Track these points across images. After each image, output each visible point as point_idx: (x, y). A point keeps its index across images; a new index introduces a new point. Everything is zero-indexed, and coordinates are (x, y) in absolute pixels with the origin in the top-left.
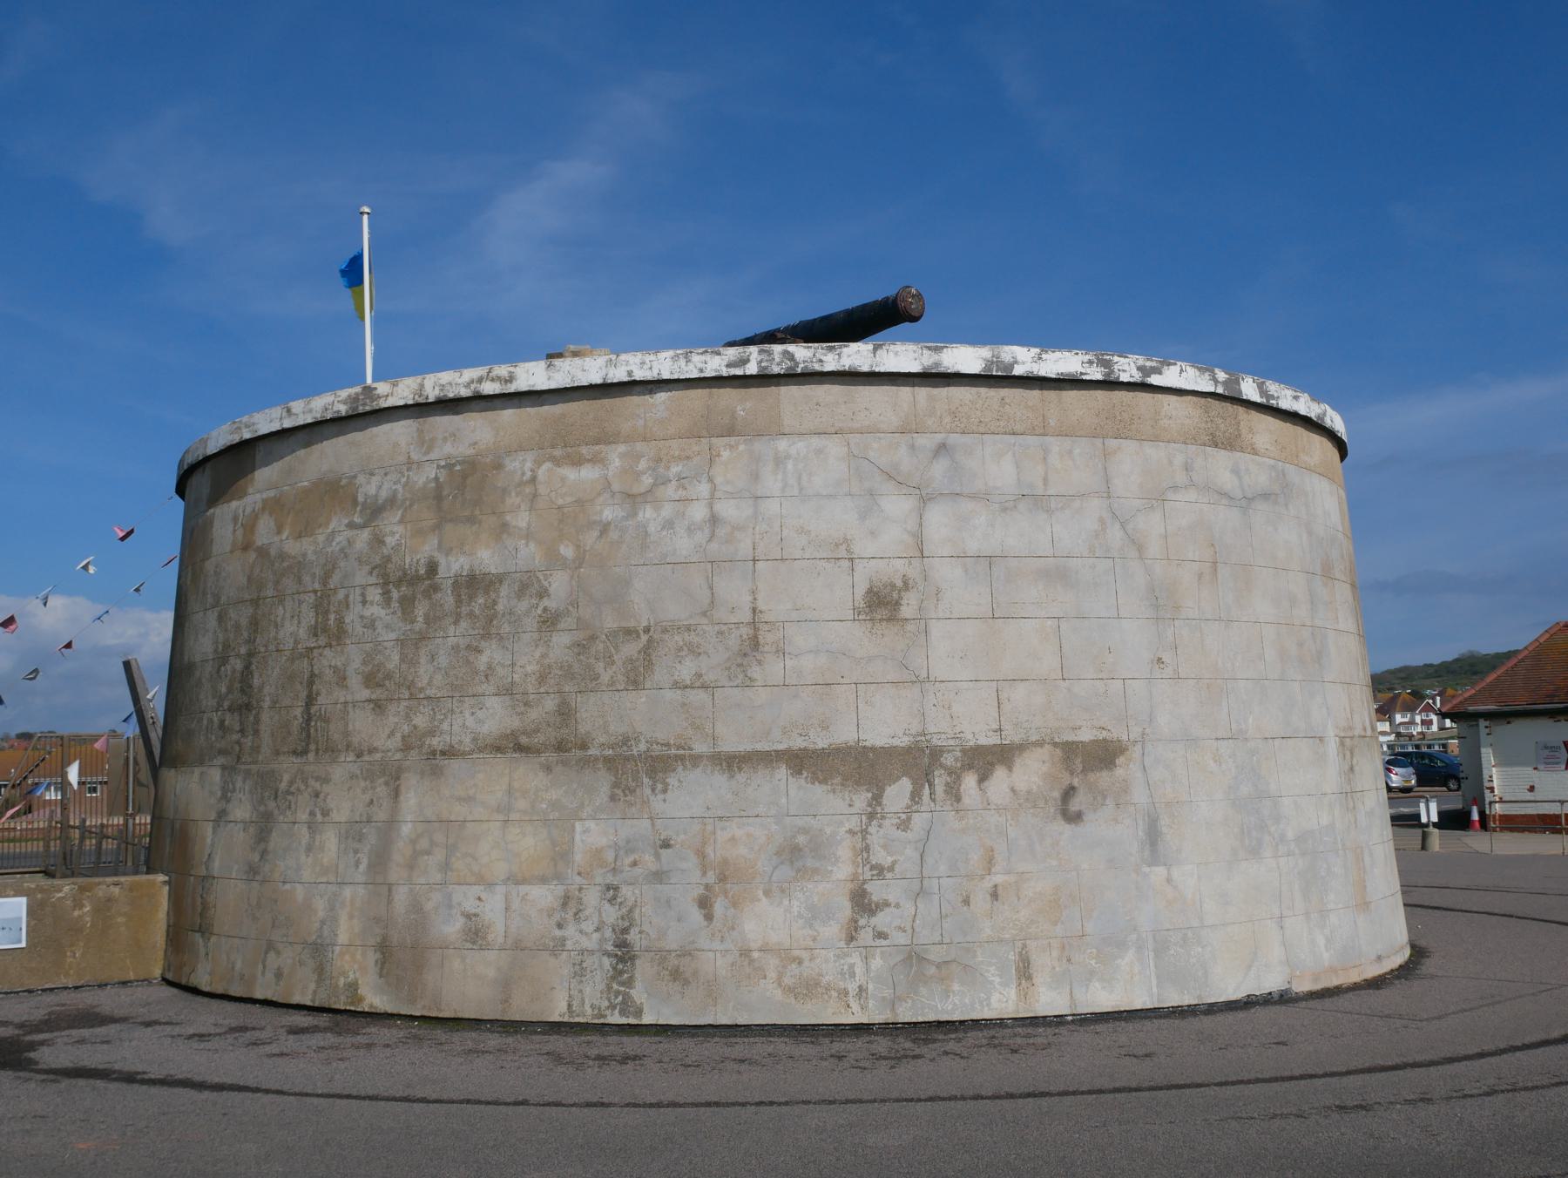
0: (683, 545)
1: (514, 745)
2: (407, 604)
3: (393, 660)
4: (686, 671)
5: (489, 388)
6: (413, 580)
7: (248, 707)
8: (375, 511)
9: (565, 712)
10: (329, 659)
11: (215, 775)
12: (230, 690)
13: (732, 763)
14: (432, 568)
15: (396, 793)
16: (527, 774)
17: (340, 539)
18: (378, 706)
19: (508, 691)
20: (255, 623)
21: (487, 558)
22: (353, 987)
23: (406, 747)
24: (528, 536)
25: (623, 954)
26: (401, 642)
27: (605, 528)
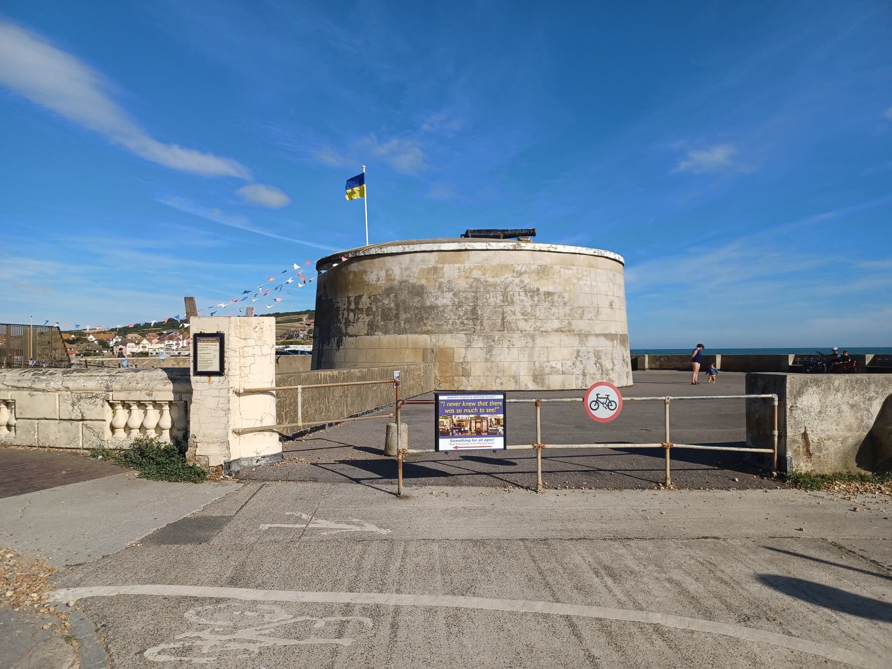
0: (587, 290)
1: (559, 330)
2: (532, 297)
3: (529, 310)
4: (589, 316)
5: (551, 249)
6: (534, 292)
7: (477, 319)
8: (521, 274)
9: (570, 323)
10: (508, 309)
11: (462, 336)
12: (466, 313)
13: (597, 335)
14: (538, 290)
15: (534, 340)
16: (563, 337)
17: (511, 279)
18: (526, 320)
19: (558, 318)
20: (476, 298)
21: (551, 289)
22: (526, 385)
23: (535, 330)
24: (559, 284)
25: (584, 375)
26: (531, 306)
27: (574, 284)
